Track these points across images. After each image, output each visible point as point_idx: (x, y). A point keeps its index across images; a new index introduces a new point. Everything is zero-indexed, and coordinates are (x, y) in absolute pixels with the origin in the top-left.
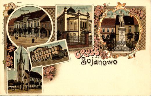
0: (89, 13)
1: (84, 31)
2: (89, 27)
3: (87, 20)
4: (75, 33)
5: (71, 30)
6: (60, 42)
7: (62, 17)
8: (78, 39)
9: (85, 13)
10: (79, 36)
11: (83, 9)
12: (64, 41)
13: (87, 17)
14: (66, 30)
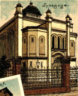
0: (71, 16)
1: (59, 56)
2: (70, 49)
3: (66, 32)
4: (40, 61)
5: (31, 56)
6: (7, 81)
7: (11, 25)
8: (48, 75)
9: (63, 16)
10: (50, 68)
11: (59, 8)
12: (17, 79)
13: (67, 26)
14: (20, 54)
